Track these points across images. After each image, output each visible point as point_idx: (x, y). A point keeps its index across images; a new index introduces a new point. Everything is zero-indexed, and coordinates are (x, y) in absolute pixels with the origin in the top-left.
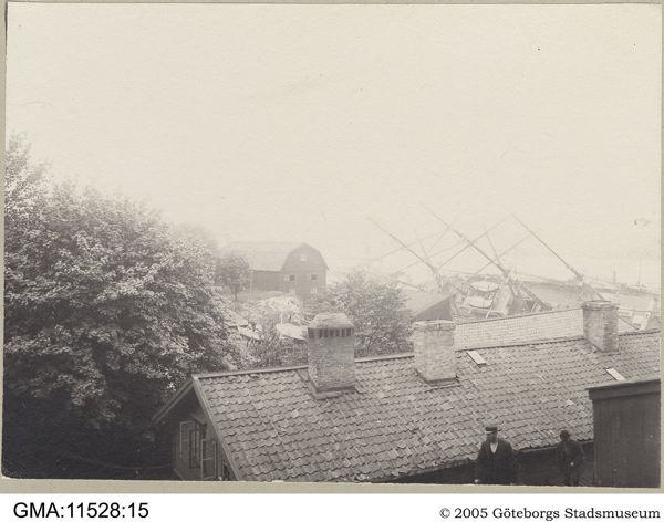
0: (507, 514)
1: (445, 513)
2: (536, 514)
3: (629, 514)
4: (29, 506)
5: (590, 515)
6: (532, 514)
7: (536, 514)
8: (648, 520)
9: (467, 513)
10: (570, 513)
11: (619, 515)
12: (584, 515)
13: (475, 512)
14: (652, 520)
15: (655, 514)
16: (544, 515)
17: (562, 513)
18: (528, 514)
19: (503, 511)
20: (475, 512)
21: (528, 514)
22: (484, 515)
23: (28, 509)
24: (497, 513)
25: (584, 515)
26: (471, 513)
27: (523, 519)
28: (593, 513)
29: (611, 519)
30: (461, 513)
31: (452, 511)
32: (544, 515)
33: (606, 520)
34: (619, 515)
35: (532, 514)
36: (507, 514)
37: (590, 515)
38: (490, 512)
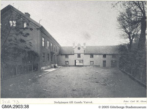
0: (113, 107)
1: (100, 107)
2: (119, 107)
3: (139, 107)
4: (5, 105)
5: (131, 107)
6: (118, 107)
7: (119, 107)
8: (144, 108)
9: (104, 107)
10: (127, 107)
11: (137, 107)
12: (130, 107)
13: (106, 107)
14: (144, 108)
15: (145, 107)
16: (121, 107)
17: (125, 107)
18: (118, 107)
19: (112, 107)
20: (106, 107)
21: (118, 107)
22: (108, 107)
23: (5, 106)
24: (111, 107)
25: (130, 107)
26: (105, 107)
27: (117, 108)
28: (132, 107)
29: (136, 108)
30: (103, 107)
31: (101, 106)
32: (121, 107)
33: (135, 108)
34: (137, 107)
35: (118, 107)
36: (113, 107)
37: (131, 107)
38: (109, 107)
